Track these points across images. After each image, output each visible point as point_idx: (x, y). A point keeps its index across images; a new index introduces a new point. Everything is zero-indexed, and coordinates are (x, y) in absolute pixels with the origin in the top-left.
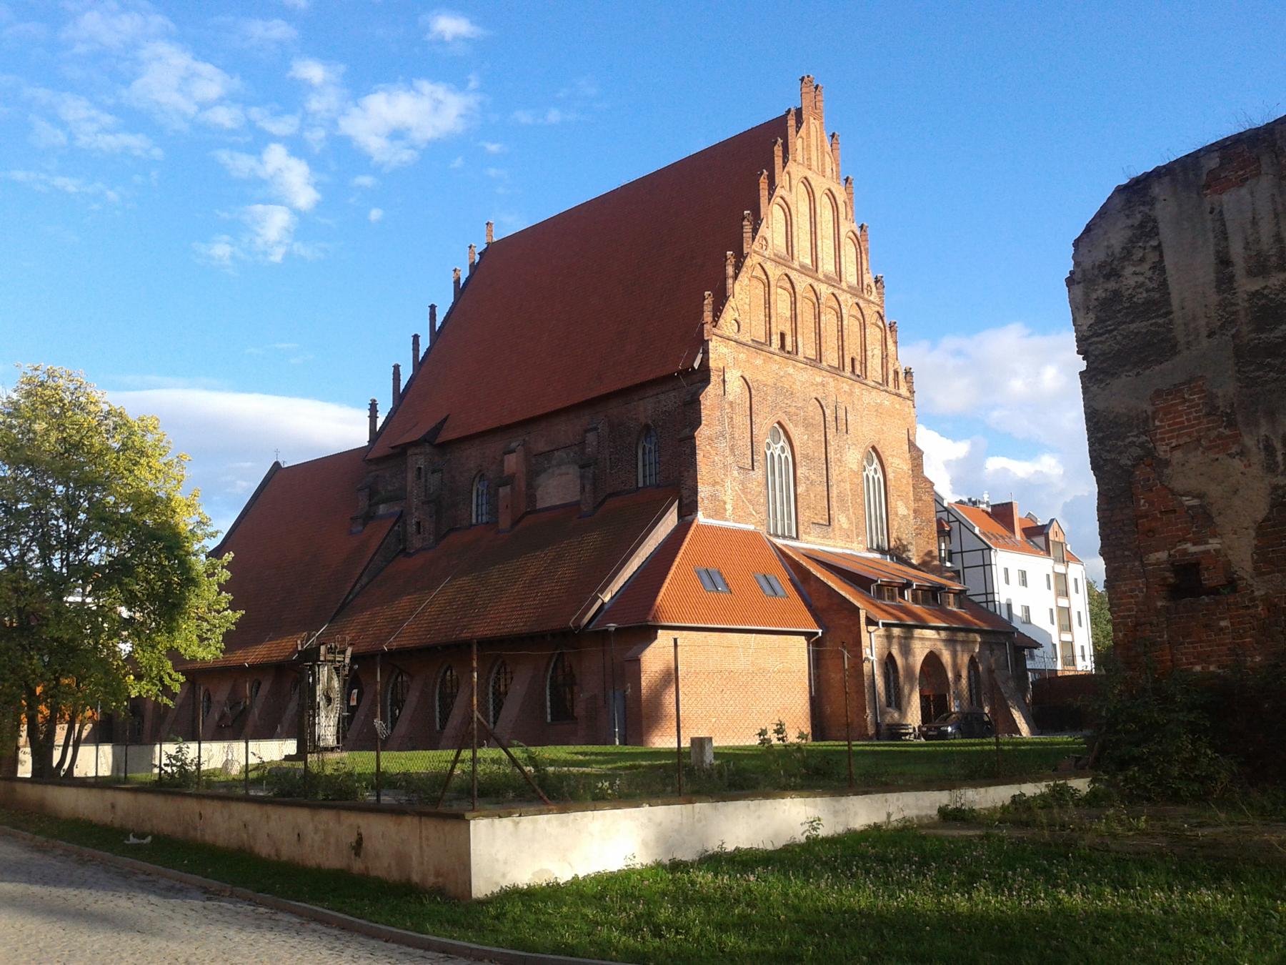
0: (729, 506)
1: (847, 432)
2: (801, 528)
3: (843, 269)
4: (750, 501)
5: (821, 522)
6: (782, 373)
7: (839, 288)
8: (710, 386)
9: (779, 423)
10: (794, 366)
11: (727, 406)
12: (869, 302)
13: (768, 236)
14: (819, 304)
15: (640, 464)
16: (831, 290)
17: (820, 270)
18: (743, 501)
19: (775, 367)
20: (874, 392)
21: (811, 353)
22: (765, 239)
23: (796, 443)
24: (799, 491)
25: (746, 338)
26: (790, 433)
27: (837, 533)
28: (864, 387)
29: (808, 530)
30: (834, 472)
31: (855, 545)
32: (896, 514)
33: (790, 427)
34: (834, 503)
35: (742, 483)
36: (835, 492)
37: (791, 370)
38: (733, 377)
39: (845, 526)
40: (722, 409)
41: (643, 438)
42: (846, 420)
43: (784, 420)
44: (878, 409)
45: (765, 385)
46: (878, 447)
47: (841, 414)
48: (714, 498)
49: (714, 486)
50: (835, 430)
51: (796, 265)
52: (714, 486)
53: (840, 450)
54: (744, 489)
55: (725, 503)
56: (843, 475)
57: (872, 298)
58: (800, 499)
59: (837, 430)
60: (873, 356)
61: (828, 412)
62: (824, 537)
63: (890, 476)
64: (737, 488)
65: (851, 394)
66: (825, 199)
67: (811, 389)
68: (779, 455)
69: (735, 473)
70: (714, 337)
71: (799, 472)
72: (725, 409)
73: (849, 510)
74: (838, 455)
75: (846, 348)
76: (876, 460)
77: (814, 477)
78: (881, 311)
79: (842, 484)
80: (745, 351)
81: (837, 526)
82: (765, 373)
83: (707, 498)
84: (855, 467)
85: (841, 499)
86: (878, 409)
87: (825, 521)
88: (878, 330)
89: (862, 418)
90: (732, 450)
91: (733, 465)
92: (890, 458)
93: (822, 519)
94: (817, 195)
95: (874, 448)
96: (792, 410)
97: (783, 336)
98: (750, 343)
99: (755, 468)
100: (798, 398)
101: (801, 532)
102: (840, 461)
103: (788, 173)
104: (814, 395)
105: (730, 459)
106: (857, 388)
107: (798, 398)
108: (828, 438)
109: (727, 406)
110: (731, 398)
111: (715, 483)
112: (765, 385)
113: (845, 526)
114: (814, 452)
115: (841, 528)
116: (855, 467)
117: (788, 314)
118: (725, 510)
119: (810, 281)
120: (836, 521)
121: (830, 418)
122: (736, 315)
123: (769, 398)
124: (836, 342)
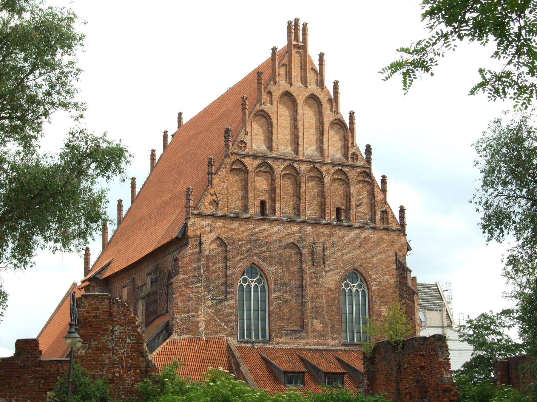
0: (202, 326)
1: (324, 263)
2: (273, 333)
4: (222, 320)
5: (295, 328)
6: (257, 230)
8: (188, 248)
11: (203, 259)
13: (247, 139)
17: (301, 153)
18: (215, 320)
19: (251, 227)
20: (357, 231)
21: (290, 211)
24: (271, 308)
25: (225, 212)
27: (311, 334)
30: (310, 292)
31: (329, 341)
32: (380, 315)
35: (216, 309)
38: (208, 239)
40: (198, 262)
42: (324, 255)
43: (258, 262)
45: (240, 241)
46: (361, 270)
48: (188, 321)
49: (188, 313)
52: (188, 313)
53: (316, 276)
54: (217, 312)
55: (198, 323)
59: (313, 262)
61: (305, 251)
63: (374, 288)
64: (210, 312)
67: (287, 237)
69: (209, 303)
72: (201, 262)
73: (324, 317)
74: (315, 280)
78: (368, 171)
79: (317, 300)
81: (310, 329)
83: (182, 322)
84: (333, 287)
86: (362, 243)
88: (366, 184)
93: (296, 325)
94: (300, 102)
96: (267, 253)
97: (263, 204)
98: (227, 214)
100: (273, 245)
103: (270, 93)
104: (290, 241)
107: (273, 245)
108: (304, 269)
109: (203, 259)
110: (207, 253)
111: (189, 311)
112: (240, 241)
115: (314, 331)
119: (290, 163)
120: (310, 326)
122: (214, 198)
123: (244, 249)
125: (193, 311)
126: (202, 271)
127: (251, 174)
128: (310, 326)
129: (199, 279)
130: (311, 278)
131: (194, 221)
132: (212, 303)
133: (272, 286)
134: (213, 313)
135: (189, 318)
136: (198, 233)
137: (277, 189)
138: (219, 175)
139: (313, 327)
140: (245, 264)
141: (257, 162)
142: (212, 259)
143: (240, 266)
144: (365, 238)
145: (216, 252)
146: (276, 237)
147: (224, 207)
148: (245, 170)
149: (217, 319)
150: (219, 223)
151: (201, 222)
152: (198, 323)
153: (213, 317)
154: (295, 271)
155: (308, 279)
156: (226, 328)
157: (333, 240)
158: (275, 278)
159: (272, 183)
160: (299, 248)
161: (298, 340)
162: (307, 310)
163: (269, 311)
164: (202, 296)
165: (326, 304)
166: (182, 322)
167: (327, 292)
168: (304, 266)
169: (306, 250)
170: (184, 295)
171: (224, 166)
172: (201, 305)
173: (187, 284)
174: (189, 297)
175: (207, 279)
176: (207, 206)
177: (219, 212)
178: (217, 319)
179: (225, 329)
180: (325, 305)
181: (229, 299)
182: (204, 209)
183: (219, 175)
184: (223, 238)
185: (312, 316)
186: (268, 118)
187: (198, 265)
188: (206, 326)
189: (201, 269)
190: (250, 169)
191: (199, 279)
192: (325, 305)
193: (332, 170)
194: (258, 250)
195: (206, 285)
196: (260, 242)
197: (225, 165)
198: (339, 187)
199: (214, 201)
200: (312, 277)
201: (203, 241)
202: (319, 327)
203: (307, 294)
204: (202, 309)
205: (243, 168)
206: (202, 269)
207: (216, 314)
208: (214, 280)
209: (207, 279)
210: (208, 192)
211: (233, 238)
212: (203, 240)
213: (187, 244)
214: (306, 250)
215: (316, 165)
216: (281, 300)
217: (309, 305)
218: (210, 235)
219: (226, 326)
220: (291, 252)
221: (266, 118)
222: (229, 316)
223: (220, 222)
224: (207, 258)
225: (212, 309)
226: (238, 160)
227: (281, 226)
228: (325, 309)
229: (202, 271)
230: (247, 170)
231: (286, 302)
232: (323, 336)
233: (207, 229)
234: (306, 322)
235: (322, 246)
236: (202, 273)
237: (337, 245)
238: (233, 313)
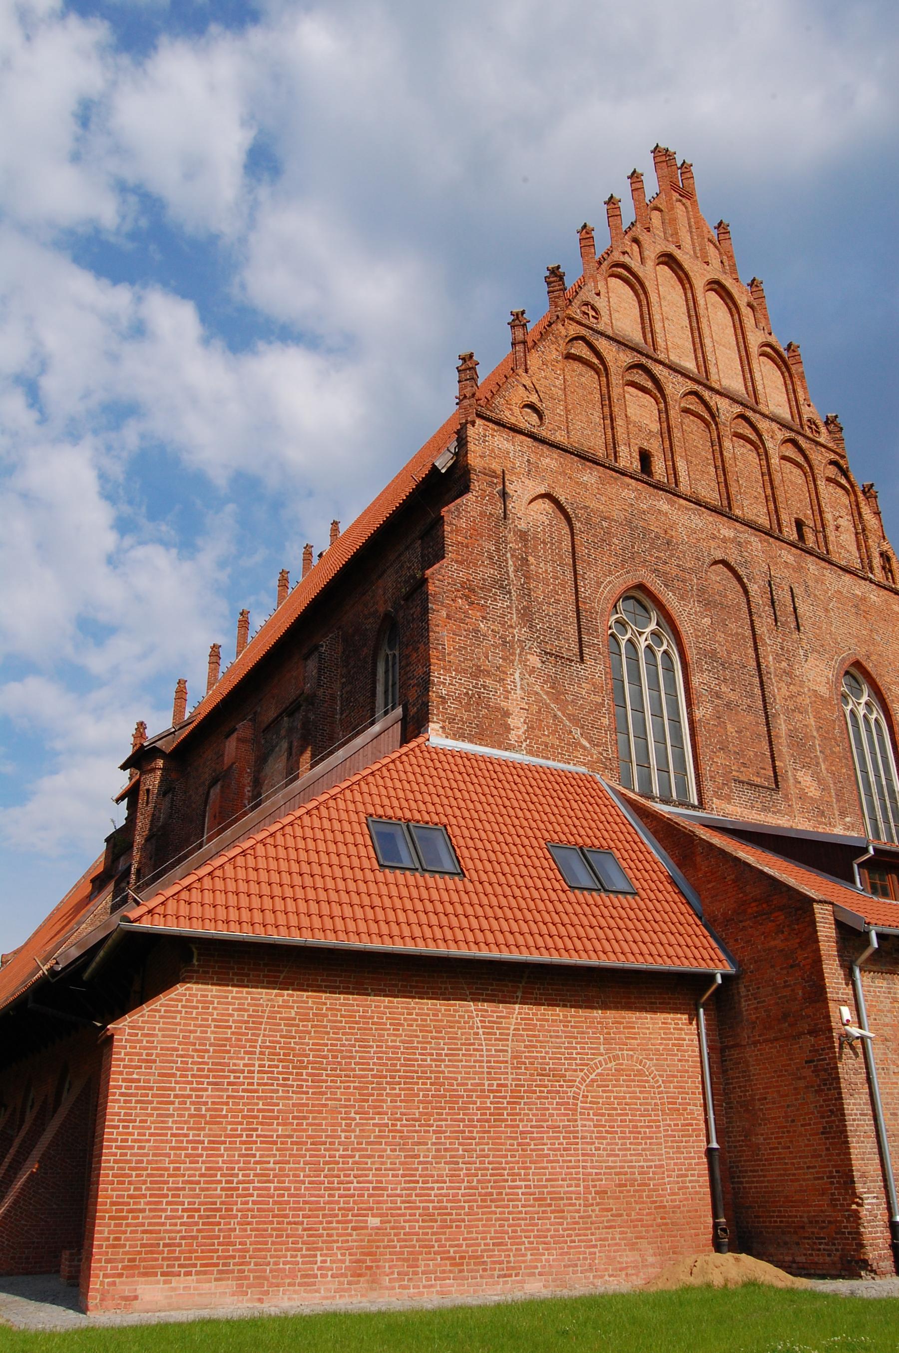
2: (708, 785)
3: (760, 388)
5: (757, 780)
7: (755, 411)
8: (469, 496)
9: (641, 587)
10: (671, 503)
12: (818, 444)
14: (716, 424)
15: (380, 689)
16: (738, 409)
20: (847, 578)
22: (594, 308)
23: (686, 629)
24: (698, 714)
26: (668, 607)
27: (797, 806)
28: (823, 564)
29: (726, 790)
30: (778, 690)
33: (670, 599)
34: (783, 747)
36: (783, 727)
37: (665, 507)
39: (813, 791)
40: (501, 541)
41: (386, 647)
42: (795, 609)
44: (860, 606)
45: (605, 519)
46: (870, 667)
47: (782, 595)
49: (475, 676)
50: (771, 621)
51: (662, 356)
52: (475, 676)
54: (559, 693)
55: (507, 714)
56: (799, 699)
57: (822, 440)
58: (702, 731)
59: (776, 620)
60: (837, 528)
61: (753, 588)
62: (765, 809)
64: (537, 688)
65: (799, 569)
66: (713, 297)
67: (713, 544)
68: (649, 647)
69: (534, 660)
70: (479, 422)
71: (695, 681)
75: (780, 499)
76: (865, 689)
77: (732, 696)
80: (555, 456)
81: (793, 791)
82: (603, 499)
83: (458, 699)
85: (799, 742)
87: (767, 779)
89: (827, 610)
90: (526, 616)
91: (529, 644)
92: (893, 687)
93: (758, 774)
95: (857, 664)
99: (586, 657)
100: (684, 552)
101: (708, 794)
102: (789, 674)
104: (719, 555)
105: (519, 633)
106: (812, 565)
107: (684, 552)
108: (758, 632)
109: (511, 537)
110: (522, 526)
111: (478, 672)
113: (813, 791)
114: (729, 652)
116: (823, 690)
117: (655, 427)
118: (508, 729)
120: (791, 781)
121: (759, 598)
122: (534, 398)
124: (760, 490)
125: (488, 674)
126: (511, 569)
127: (615, 380)
128: (791, 781)
129: (502, 587)
130: (778, 658)
131: (486, 436)
132: (543, 662)
133: (692, 654)
134: (547, 693)
135: (479, 693)
136: (496, 466)
137: (675, 430)
138: (543, 352)
139: (798, 786)
140: (620, 582)
141: (627, 358)
142: (535, 547)
143: (610, 582)
144: (864, 599)
145: (544, 531)
146: (688, 537)
147: (560, 428)
148: (600, 366)
149: (559, 714)
150: (550, 460)
151: (501, 441)
152: (507, 714)
153: (548, 706)
154: (737, 633)
155: (771, 658)
156: (588, 745)
157: (804, 581)
158: (697, 637)
159: (664, 414)
160: (739, 579)
161: (770, 814)
162: (781, 737)
163: (691, 722)
164: (514, 637)
165: (818, 731)
166: (458, 699)
167: (815, 702)
168: (757, 625)
169: (756, 587)
170: (462, 621)
171: (553, 339)
172: (512, 661)
173: (469, 591)
174: (477, 631)
175: (526, 593)
176: (517, 410)
177: (544, 433)
178: (559, 714)
179: (584, 748)
180: (815, 734)
181: (589, 662)
182: (507, 413)
183: (543, 352)
184: (562, 499)
185: (793, 755)
186: (638, 287)
187: (498, 550)
188: (530, 728)
189: (506, 561)
190: (613, 369)
191: (502, 587)
192: (815, 734)
193: (781, 435)
194: (652, 556)
195: (524, 608)
196: (653, 535)
197: (556, 338)
198: (795, 476)
199: (531, 406)
200: (777, 655)
201: (511, 493)
202: (812, 789)
203: (774, 696)
204: (517, 675)
205: (596, 361)
206: (510, 563)
207: (556, 700)
208: (541, 603)
209: (526, 593)
210: (517, 380)
211: (586, 507)
212: (510, 488)
213: (466, 489)
214: (756, 587)
215: (749, 414)
216: (718, 697)
217: (782, 727)
218: (527, 482)
219: (586, 739)
220: (724, 585)
221: (632, 287)
222: (591, 711)
223: (552, 459)
224: (523, 536)
225: (545, 682)
226: (583, 338)
227: (694, 514)
228: (817, 742)
229: (511, 569)
230: (606, 369)
231: (728, 705)
232: (822, 813)
233: (520, 464)
234: (782, 768)
235: (787, 588)
236: (512, 575)
237: (815, 595)
238: (603, 705)
